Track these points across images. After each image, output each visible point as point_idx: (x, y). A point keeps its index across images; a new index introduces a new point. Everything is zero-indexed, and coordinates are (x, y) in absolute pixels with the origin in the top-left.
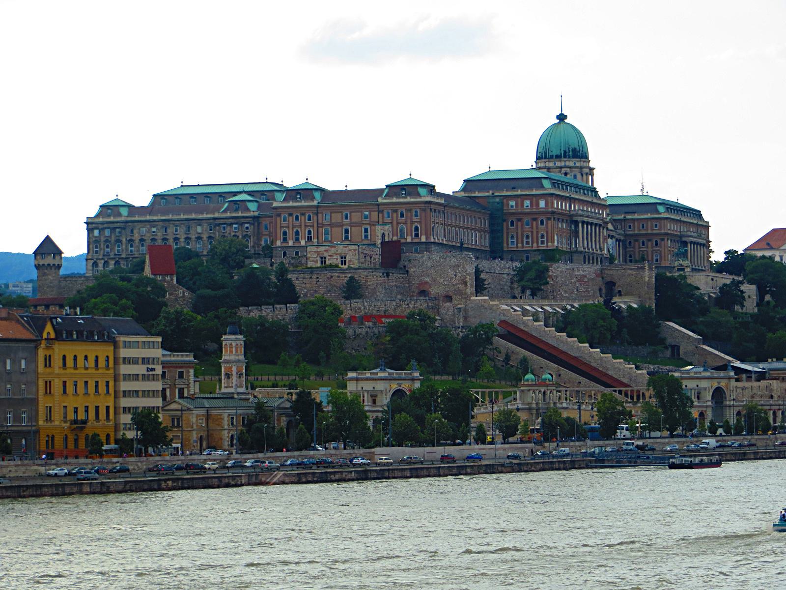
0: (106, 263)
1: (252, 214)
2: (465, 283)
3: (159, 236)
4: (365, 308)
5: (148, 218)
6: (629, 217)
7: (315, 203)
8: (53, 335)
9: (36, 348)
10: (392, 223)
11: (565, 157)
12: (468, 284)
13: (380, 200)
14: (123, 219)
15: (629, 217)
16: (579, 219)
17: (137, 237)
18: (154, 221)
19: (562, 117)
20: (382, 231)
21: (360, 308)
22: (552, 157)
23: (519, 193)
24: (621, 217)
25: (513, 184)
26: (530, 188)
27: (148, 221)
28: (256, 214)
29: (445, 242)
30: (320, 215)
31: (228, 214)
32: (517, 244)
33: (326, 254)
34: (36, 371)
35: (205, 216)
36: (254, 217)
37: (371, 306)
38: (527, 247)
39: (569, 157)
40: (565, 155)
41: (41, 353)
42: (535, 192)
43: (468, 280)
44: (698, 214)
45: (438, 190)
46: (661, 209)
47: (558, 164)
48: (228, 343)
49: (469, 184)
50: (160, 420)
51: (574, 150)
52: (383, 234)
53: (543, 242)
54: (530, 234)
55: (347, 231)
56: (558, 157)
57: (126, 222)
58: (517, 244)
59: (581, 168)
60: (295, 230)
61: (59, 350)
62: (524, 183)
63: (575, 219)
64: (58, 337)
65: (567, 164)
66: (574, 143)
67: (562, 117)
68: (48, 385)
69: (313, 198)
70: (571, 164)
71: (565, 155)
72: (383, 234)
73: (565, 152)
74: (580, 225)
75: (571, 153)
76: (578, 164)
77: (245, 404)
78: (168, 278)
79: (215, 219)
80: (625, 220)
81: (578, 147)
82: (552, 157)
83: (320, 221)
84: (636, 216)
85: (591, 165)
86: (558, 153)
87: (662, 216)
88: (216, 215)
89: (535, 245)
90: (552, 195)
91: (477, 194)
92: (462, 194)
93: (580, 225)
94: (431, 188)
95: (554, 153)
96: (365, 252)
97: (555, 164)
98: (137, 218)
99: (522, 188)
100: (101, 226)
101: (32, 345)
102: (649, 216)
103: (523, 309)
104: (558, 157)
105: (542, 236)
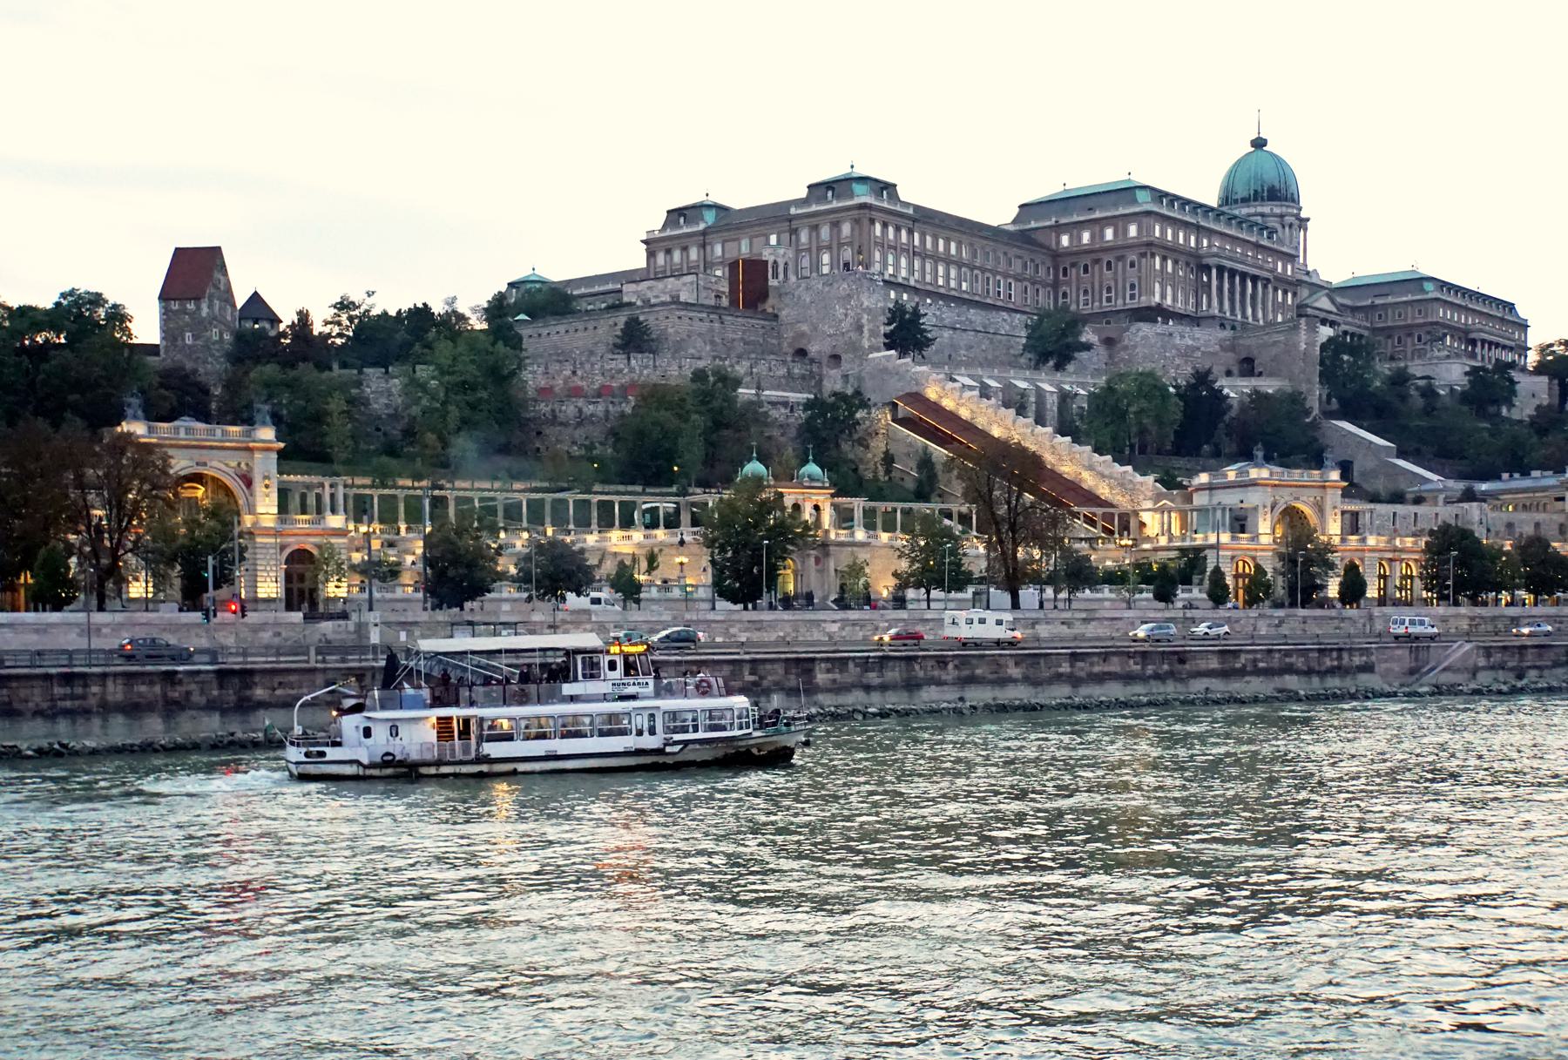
2: (859, 328)
4: (632, 370)
7: (702, 226)
12: (866, 330)
13: (793, 211)
15: (1378, 301)
16: (1212, 261)
19: (1259, 143)
21: (620, 371)
22: (1236, 201)
23: (1097, 215)
24: (1369, 302)
25: (1090, 202)
29: (912, 283)
30: (708, 248)
37: (646, 367)
40: (1256, 197)
43: (864, 321)
44: (1510, 307)
45: (903, 195)
46: (1429, 286)
50: (571, 596)
53: (1132, 297)
54: (1112, 284)
56: (1245, 200)
59: (1282, 216)
63: (1206, 261)
65: (1259, 209)
66: (1271, 177)
67: (1259, 143)
70: (1266, 210)
71: (1256, 197)
74: (1214, 272)
76: (1277, 211)
80: (1373, 307)
81: (1277, 185)
82: (1236, 201)
84: (1390, 299)
85: (1303, 215)
86: (1245, 194)
87: (1430, 296)
89: (1120, 302)
90: (1148, 213)
91: (1033, 225)
92: (1011, 228)
93: (1214, 272)
94: (885, 188)
95: (1239, 196)
96: (715, 287)
99: (1102, 207)
102: (1410, 297)
103: (982, 383)
104: (1245, 200)
105: (1132, 287)
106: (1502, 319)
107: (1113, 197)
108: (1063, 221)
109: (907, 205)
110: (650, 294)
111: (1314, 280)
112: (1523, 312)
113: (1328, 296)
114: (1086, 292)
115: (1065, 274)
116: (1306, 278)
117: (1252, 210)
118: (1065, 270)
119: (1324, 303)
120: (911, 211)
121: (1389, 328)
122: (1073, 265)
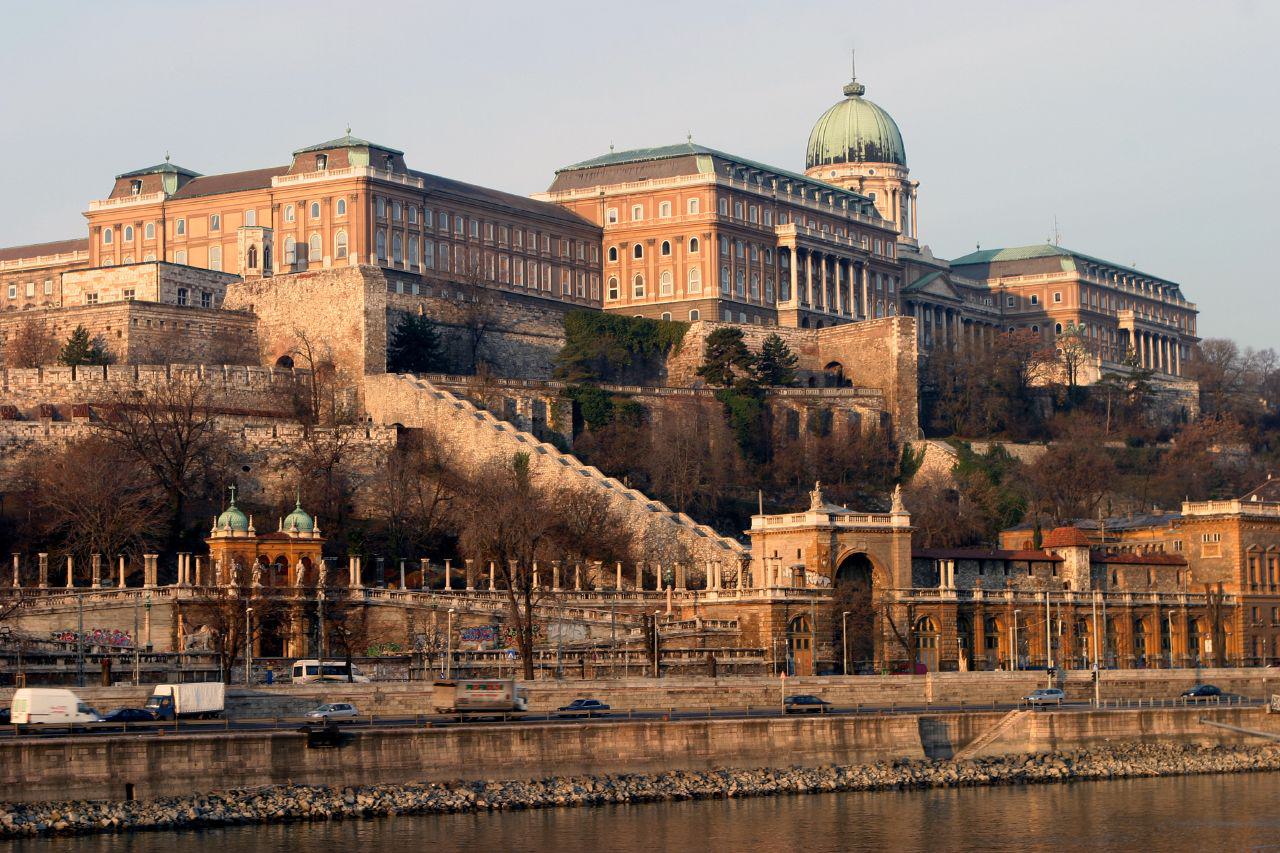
10: (296, 231)
11: (851, 159)
19: (855, 92)
20: (250, 243)
21: (63, 386)
22: (827, 162)
32: (648, 292)
39: (860, 160)
40: (853, 155)
44: (1172, 289)
45: (411, 164)
49: (565, 178)
52: (253, 247)
56: (838, 160)
58: (648, 292)
67: (855, 92)
72: (253, 247)
73: (851, 150)
75: (863, 153)
76: (878, 173)
81: (877, 142)
82: (827, 162)
83: (169, 238)
91: (574, 195)
95: (832, 155)
96: (179, 279)
97: (833, 174)
104: (838, 160)
106: (1163, 305)
108: (609, 192)
109: (415, 175)
110: (97, 288)
111: (924, 259)
112: (1190, 294)
113: (941, 277)
114: (639, 282)
115: (613, 257)
116: (915, 257)
117: (847, 172)
118: (613, 251)
119: (939, 288)
120: (420, 185)
121: (1024, 316)
122: (624, 246)
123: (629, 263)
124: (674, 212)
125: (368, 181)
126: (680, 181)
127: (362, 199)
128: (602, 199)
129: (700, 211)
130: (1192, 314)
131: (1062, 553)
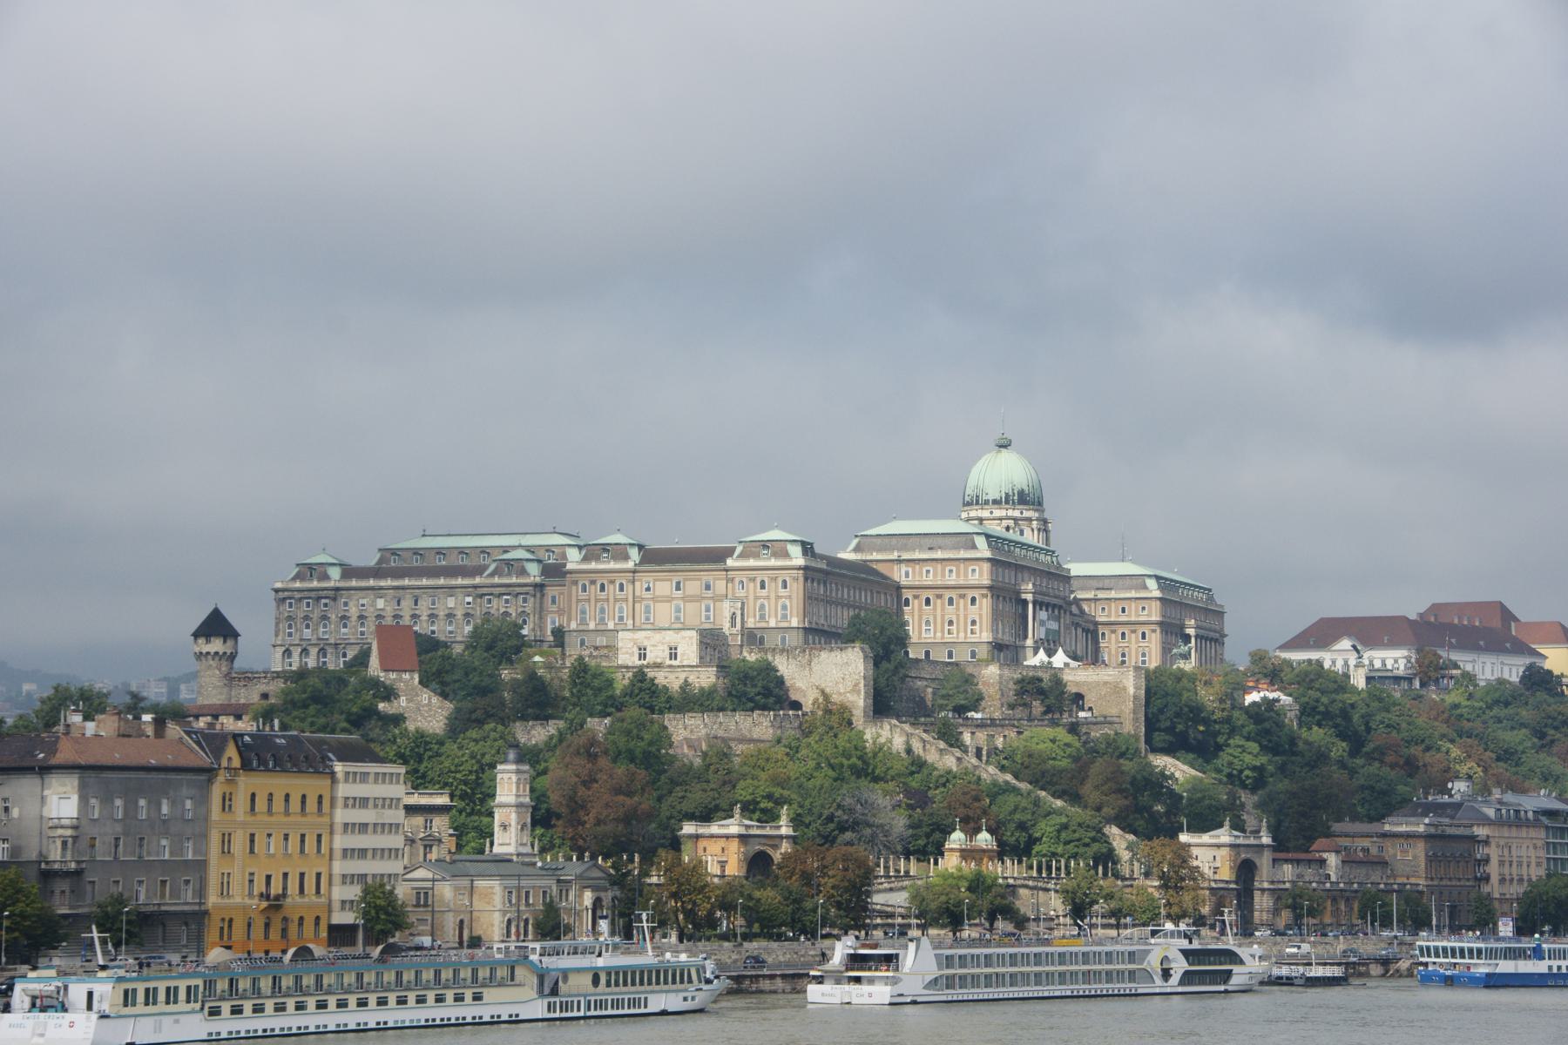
0: (305, 652)
1: (531, 580)
3: (389, 612)
5: (372, 583)
6: (1101, 595)
7: (630, 565)
8: (236, 763)
9: (210, 781)
14: (332, 584)
15: (1101, 595)
17: (353, 612)
18: (381, 588)
23: (939, 555)
25: (928, 542)
26: (956, 547)
27: (372, 589)
28: (538, 580)
30: (637, 584)
31: (496, 580)
33: (646, 643)
34: (206, 819)
35: (460, 581)
36: (536, 586)
38: (948, 638)
40: (1007, 500)
41: (217, 791)
42: (963, 554)
45: (818, 550)
47: (998, 513)
48: (506, 776)
51: (1021, 493)
55: (678, 610)
57: (337, 589)
60: (759, 603)
61: (246, 784)
62: (948, 541)
64: (246, 766)
65: (1010, 513)
68: (226, 840)
69: (626, 558)
74: (1031, 606)
77: (529, 870)
78: (406, 676)
79: (475, 587)
82: (987, 502)
84: (1113, 594)
88: (478, 580)
89: (962, 635)
95: (991, 497)
98: (354, 583)
100: (297, 595)
101: (203, 777)
102: (1133, 594)
104: (995, 502)
107: (954, 539)
109: (822, 557)
117: (1003, 513)
123: (920, 609)
124: (958, 575)
125: (805, 568)
126: (963, 554)
127: (801, 579)
128: (899, 561)
129: (981, 575)
130: (1220, 614)
131: (1325, 855)
